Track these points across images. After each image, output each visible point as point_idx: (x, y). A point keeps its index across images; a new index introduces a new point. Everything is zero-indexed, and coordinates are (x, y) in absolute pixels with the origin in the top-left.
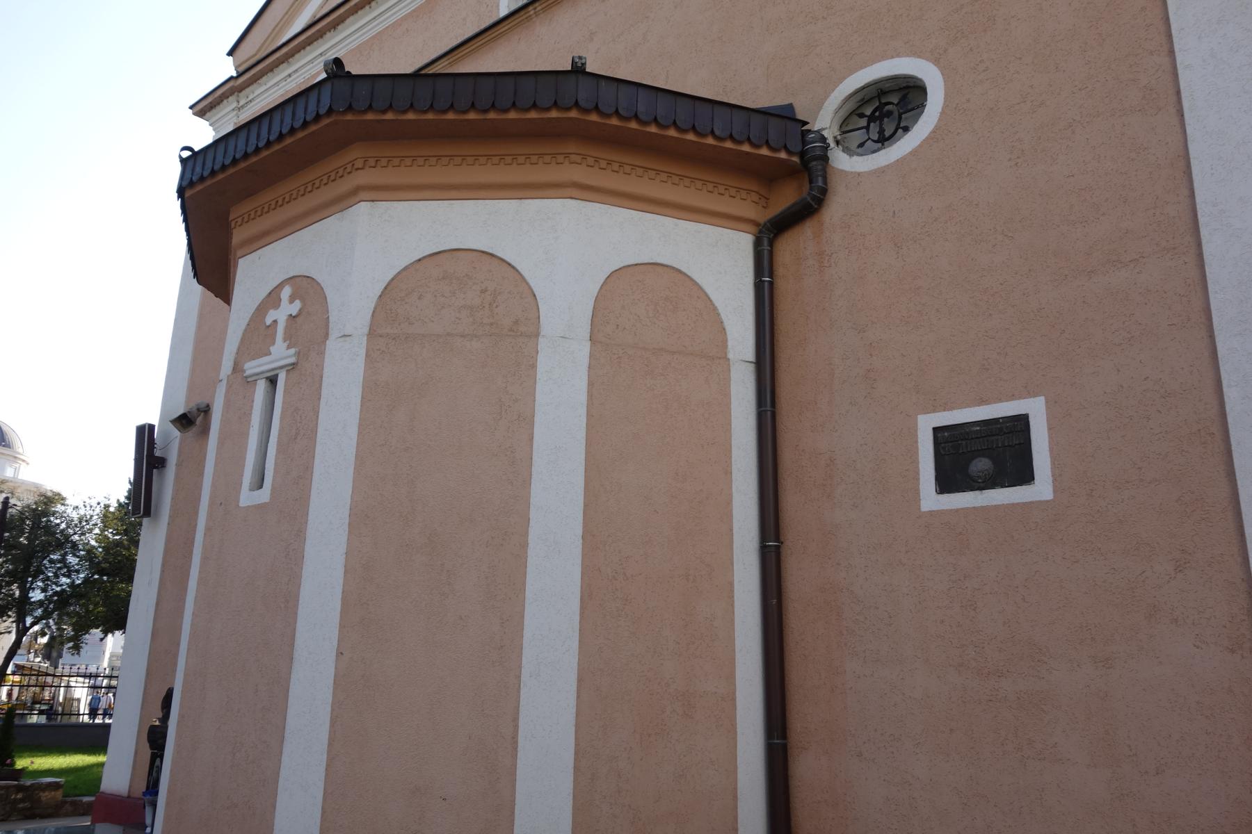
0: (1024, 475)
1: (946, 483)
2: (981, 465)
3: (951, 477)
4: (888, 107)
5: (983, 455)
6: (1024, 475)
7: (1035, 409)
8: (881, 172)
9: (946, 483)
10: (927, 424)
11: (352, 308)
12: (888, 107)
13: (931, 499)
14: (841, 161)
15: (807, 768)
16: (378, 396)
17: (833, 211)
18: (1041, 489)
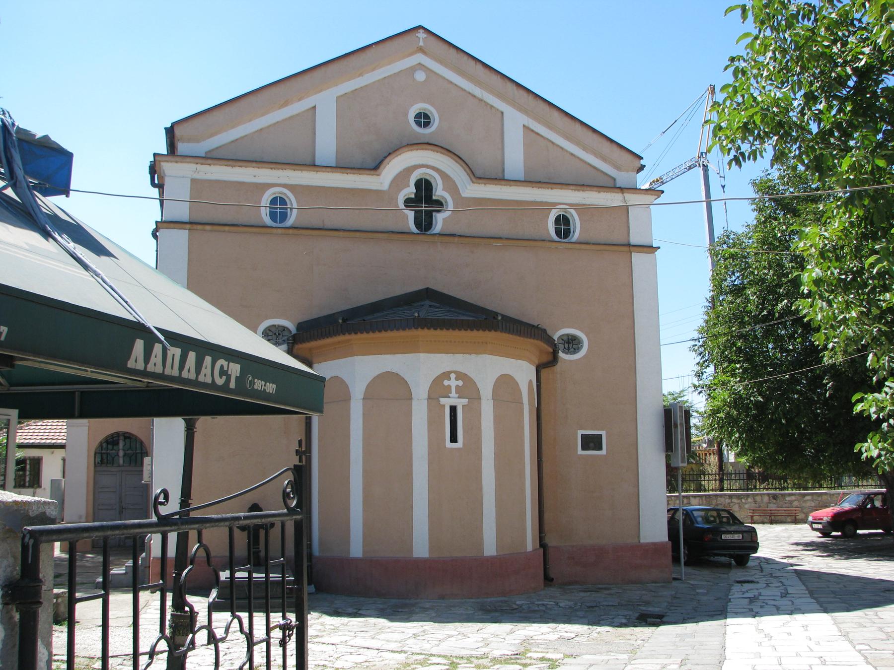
0: (600, 448)
1: (583, 448)
2: (592, 445)
3: (584, 448)
4: (572, 343)
5: (592, 442)
6: (600, 448)
7: (603, 433)
8: (571, 361)
9: (583, 448)
10: (580, 433)
11: (486, 390)
12: (572, 343)
13: (580, 452)
14: (561, 355)
15: (547, 516)
16: (498, 420)
17: (558, 367)
18: (604, 452)
